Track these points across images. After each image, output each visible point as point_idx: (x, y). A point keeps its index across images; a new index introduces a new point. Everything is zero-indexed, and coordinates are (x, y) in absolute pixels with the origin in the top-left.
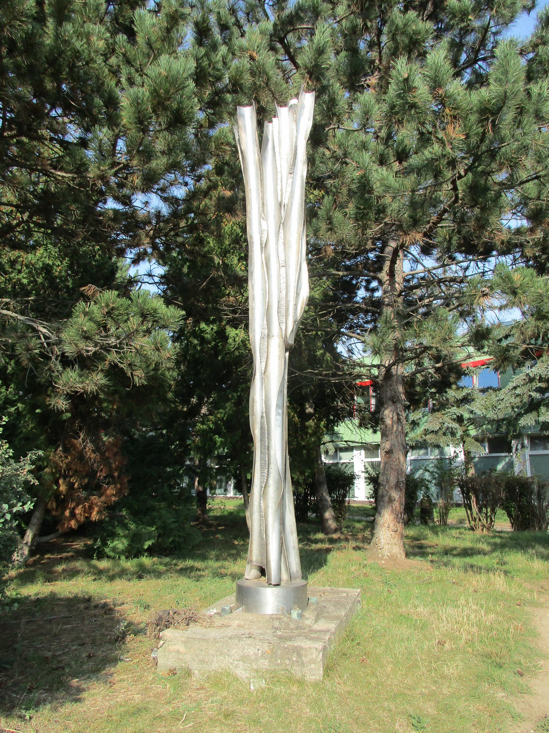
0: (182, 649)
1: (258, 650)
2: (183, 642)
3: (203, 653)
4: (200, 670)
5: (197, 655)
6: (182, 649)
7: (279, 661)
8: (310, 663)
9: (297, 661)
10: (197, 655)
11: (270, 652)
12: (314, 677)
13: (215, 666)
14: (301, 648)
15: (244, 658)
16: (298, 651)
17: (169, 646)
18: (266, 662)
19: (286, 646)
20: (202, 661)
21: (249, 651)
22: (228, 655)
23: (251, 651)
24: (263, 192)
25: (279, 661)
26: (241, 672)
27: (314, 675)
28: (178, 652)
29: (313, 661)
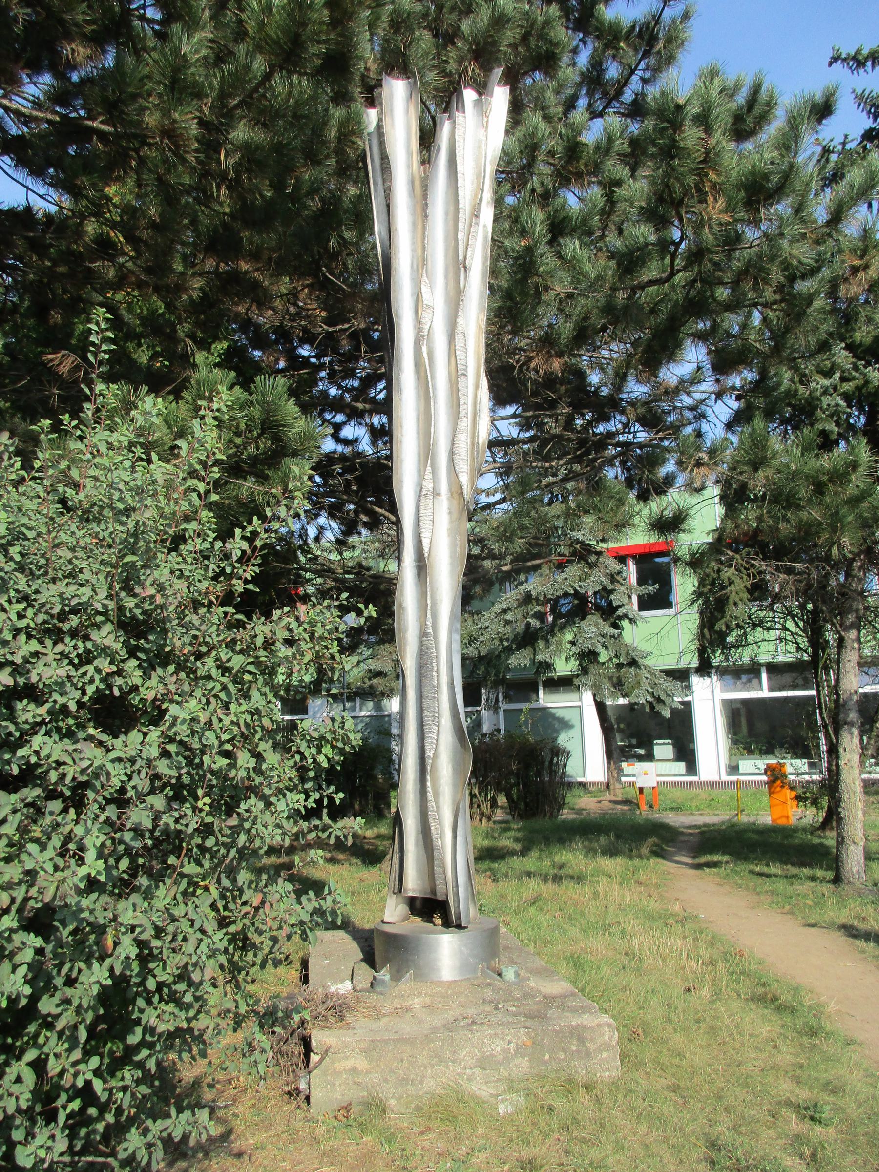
0: (361, 1063)
1: (510, 1042)
2: (362, 1051)
3: (405, 1064)
4: (401, 1097)
5: (392, 1071)
6: (361, 1063)
7: (547, 1057)
8: (601, 1052)
9: (578, 1051)
10: (392, 1071)
11: (529, 1043)
12: (607, 1074)
13: (430, 1084)
14: (585, 1027)
15: (484, 1062)
16: (579, 1034)
17: (333, 1062)
18: (525, 1062)
19: (557, 1028)
20: (404, 1081)
21: (493, 1046)
22: (454, 1062)
23: (496, 1047)
24: (425, 196)
25: (547, 1057)
26: (480, 1087)
27: (607, 1070)
28: (354, 1070)
29: (606, 1047)
